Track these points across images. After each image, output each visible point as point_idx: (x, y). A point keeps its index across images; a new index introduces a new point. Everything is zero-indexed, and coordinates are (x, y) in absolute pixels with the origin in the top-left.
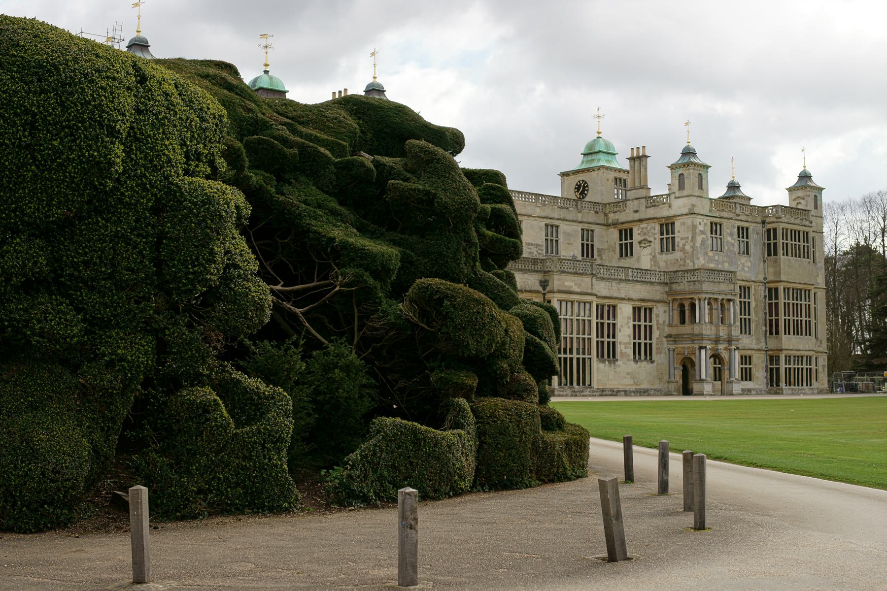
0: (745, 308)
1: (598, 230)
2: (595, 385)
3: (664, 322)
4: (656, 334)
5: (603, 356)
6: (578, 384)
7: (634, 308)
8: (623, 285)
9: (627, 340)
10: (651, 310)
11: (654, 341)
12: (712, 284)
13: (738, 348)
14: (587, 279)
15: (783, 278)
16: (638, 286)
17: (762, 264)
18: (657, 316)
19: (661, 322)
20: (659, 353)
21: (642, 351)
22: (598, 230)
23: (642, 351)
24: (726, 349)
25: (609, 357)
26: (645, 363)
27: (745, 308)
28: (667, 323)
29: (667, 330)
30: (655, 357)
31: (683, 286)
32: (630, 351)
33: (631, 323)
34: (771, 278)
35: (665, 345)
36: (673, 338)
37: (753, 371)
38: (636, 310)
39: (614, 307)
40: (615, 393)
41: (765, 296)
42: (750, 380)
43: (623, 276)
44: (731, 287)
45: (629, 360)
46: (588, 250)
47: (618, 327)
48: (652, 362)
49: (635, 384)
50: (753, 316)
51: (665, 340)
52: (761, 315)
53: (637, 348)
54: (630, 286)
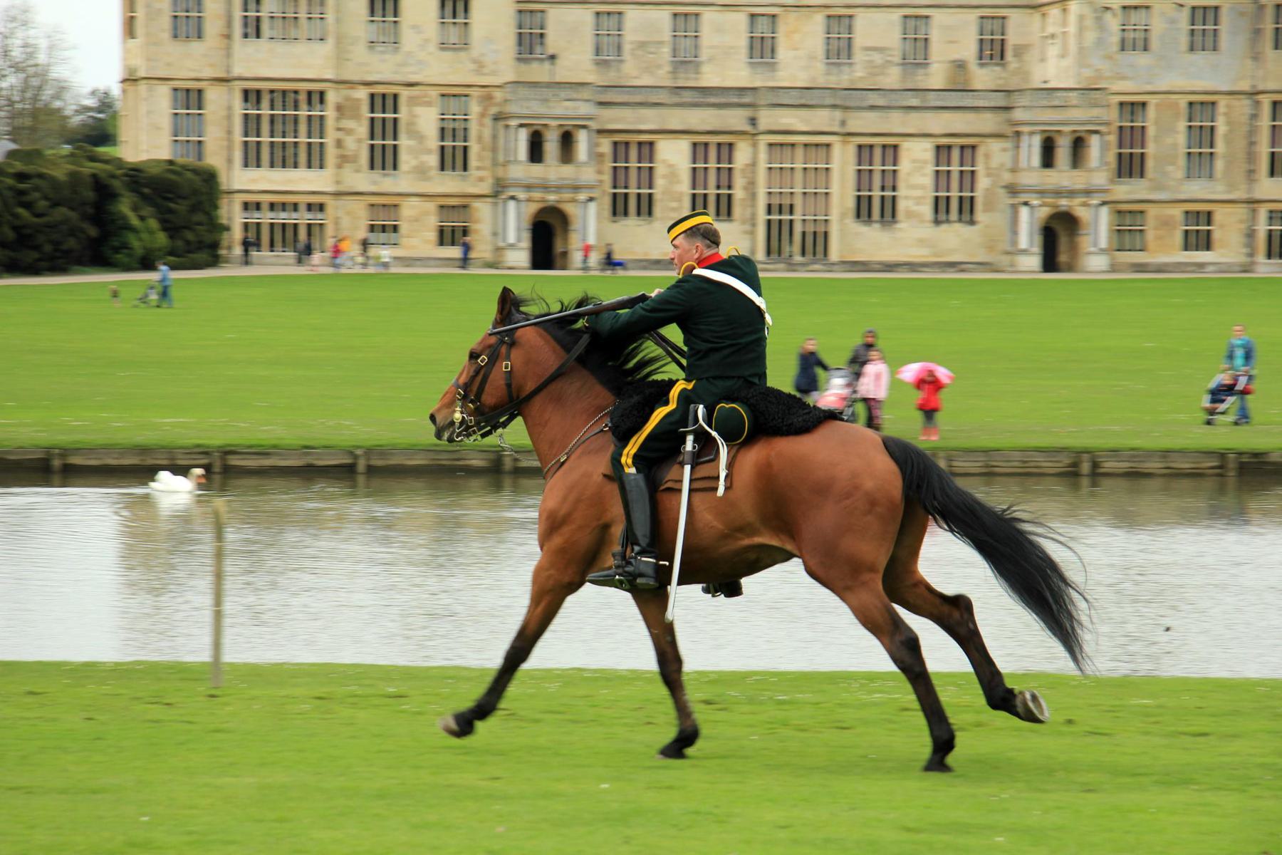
0: (1203, 136)
1: (1015, 17)
2: (834, 255)
3: (1002, 165)
4: (983, 183)
5: (870, 215)
6: (803, 253)
7: (938, 148)
8: (914, 115)
9: (918, 193)
10: (974, 147)
11: (979, 194)
12: (1049, 110)
13: (1104, 203)
14: (824, 113)
15: (1271, 86)
16: (947, 115)
17: (1249, 62)
18: (987, 156)
19: (995, 163)
20: (989, 207)
21: (955, 205)
22: (1015, 17)
23: (955, 205)
24: (1085, 205)
25: (882, 215)
26: (958, 226)
27: (1203, 136)
28: (1009, 164)
29: (1007, 177)
30: (980, 215)
31: (1018, 115)
32: (927, 210)
33: (930, 169)
34: (1261, 88)
35: (1005, 200)
36: (1013, 190)
37: (1217, 235)
38: (942, 152)
39: (895, 147)
40: (890, 267)
41: (1254, 117)
42: (1208, 247)
43: (914, 102)
44: (1095, 113)
45: (923, 221)
46: (994, 50)
47: (902, 176)
48: (972, 222)
49: (935, 255)
50: (1220, 148)
51: (1002, 191)
52: (1241, 144)
53: (940, 208)
54: (929, 115)
